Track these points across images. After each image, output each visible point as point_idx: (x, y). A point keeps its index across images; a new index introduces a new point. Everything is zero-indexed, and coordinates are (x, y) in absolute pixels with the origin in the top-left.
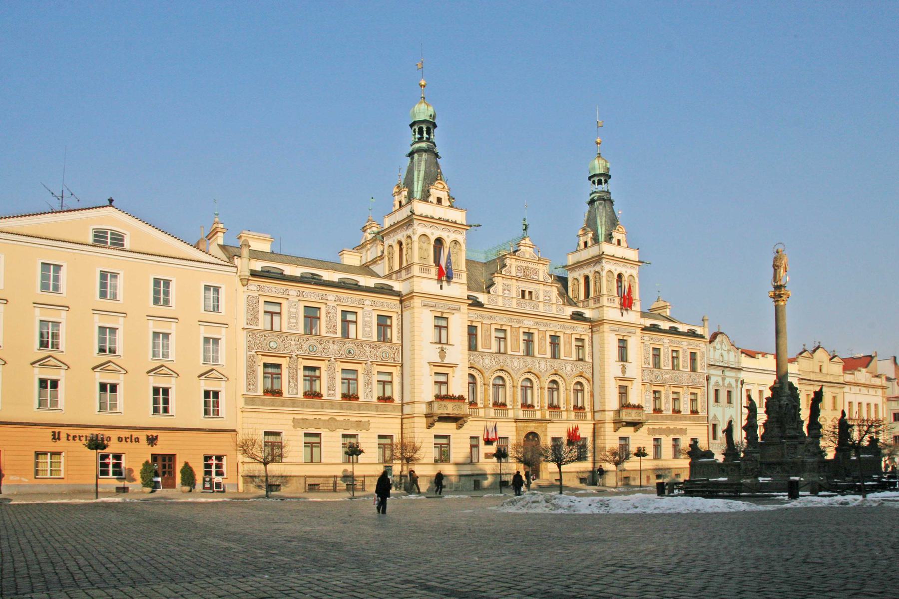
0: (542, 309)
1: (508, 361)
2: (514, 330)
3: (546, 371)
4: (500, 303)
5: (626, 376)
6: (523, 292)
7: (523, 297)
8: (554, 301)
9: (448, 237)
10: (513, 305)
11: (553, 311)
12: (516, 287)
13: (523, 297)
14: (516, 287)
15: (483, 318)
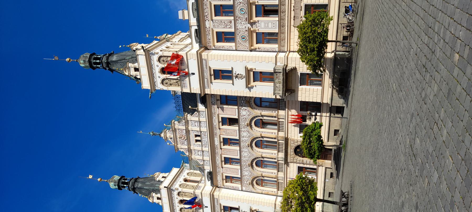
0: (205, 129)
1: (245, 159)
2: (223, 153)
3: (248, 132)
4: (207, 158)
5: (244, 74)
6: (197, 141)
7: (199, 141)
8: (197, 119)
9: (177, 198)
10: (207, 149)
11: (204, 119)
12: (195, 146)
13: (199, 141)
14: (195, 146)
15: (219, 171)
